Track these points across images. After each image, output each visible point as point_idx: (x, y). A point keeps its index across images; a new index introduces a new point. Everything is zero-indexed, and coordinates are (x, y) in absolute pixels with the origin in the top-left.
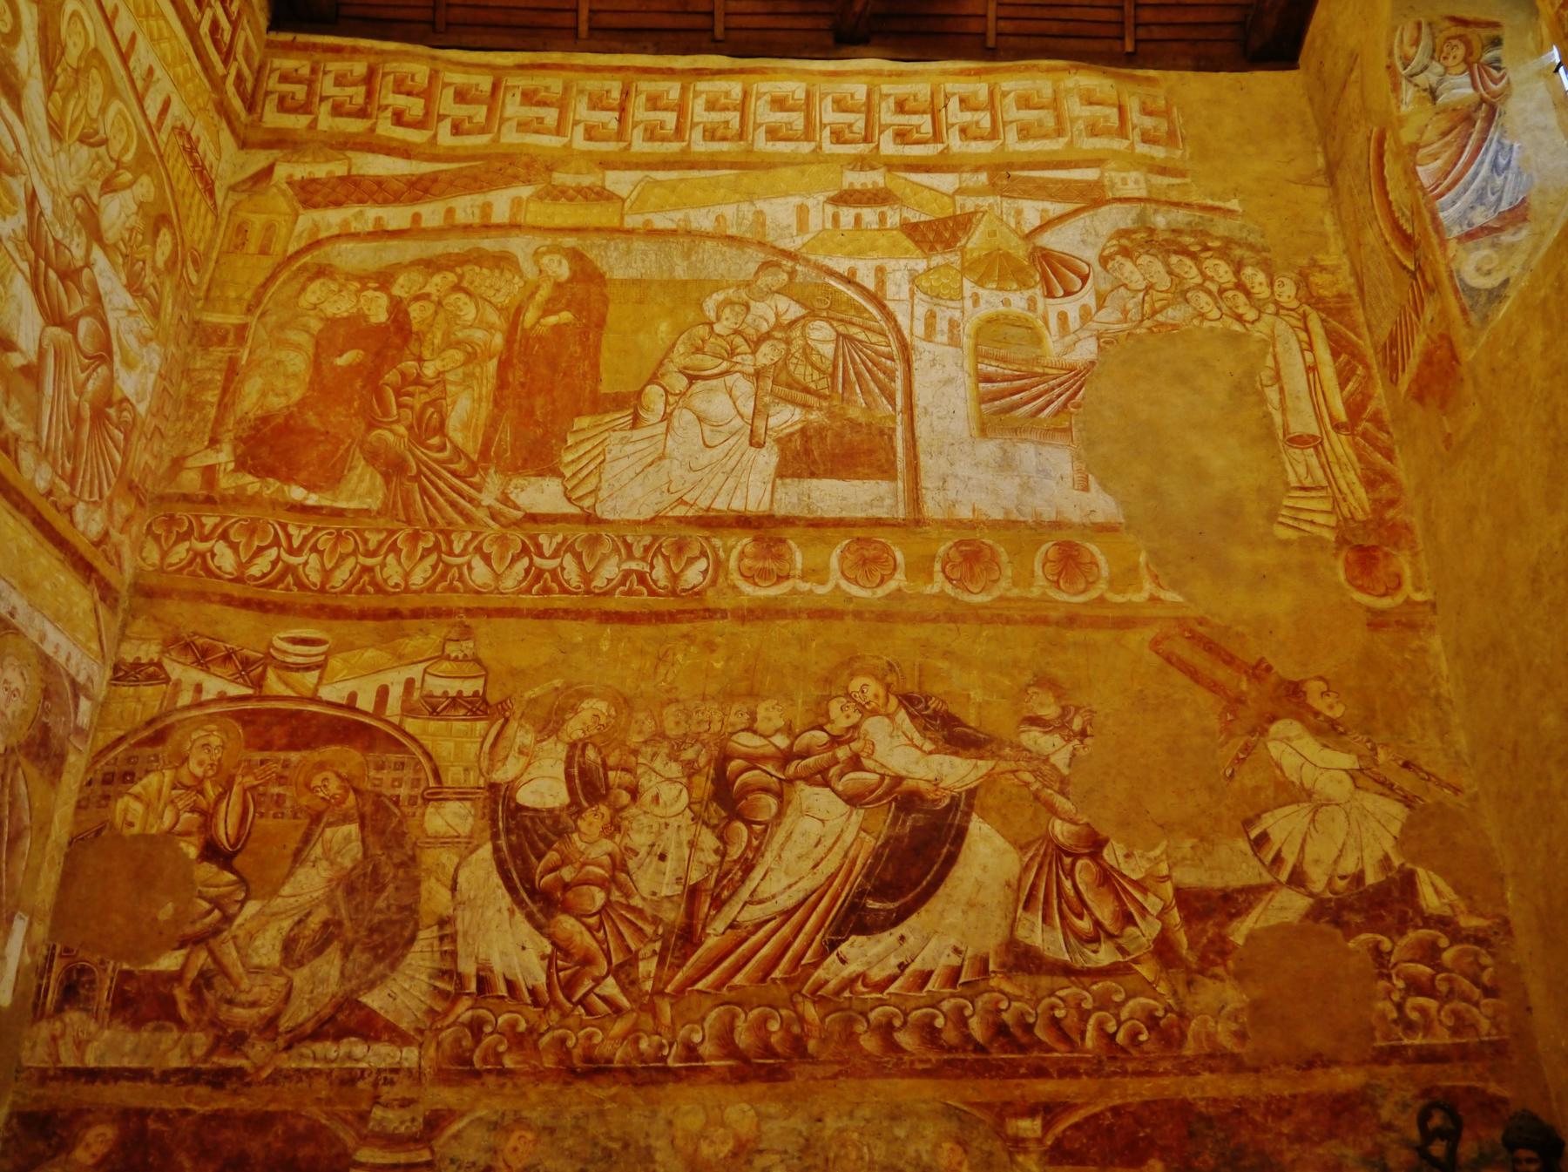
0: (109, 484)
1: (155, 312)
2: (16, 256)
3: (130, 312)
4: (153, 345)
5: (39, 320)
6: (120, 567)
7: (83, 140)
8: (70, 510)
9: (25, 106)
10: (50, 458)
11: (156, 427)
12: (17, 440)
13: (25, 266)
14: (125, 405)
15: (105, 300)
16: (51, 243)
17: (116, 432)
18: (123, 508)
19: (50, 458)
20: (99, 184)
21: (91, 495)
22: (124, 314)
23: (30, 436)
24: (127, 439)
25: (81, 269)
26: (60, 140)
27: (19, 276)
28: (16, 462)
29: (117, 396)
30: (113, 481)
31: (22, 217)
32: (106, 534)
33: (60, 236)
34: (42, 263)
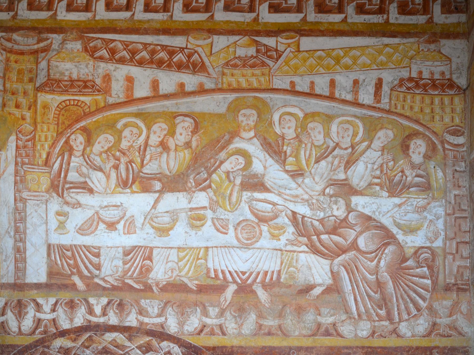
0: (424, 299)
1: (426, 187)
2: (295, 248)
3: (400, 206)
4: (433, 204)
5: (325, 263)
6: (460, 334)
7: (317, 161)
8: (395, 331)
9: (268, 184)
10: (365, 317)
11: (458, 243)
12: (334, 325)
13: (304, 248)
14: (420, 252)
15: (376, 216)
16: (316, 223)
17: (418, 270)
18: (443, 305)
19: (365, 317)
20: (342, 168)
21: (409, 314)
22: (396, 209)
23: (344, 317)
24: (429, 267)
25: (347, 216)
26: (302, 175)
27: (302, 256)
28: (339, 335)
29: (409, 252)
30: (428, 295)
31: (291, 229)
32: (434, 324)
33: (322, 215)
34: (315, 237)
